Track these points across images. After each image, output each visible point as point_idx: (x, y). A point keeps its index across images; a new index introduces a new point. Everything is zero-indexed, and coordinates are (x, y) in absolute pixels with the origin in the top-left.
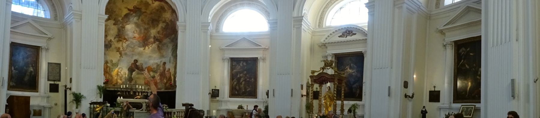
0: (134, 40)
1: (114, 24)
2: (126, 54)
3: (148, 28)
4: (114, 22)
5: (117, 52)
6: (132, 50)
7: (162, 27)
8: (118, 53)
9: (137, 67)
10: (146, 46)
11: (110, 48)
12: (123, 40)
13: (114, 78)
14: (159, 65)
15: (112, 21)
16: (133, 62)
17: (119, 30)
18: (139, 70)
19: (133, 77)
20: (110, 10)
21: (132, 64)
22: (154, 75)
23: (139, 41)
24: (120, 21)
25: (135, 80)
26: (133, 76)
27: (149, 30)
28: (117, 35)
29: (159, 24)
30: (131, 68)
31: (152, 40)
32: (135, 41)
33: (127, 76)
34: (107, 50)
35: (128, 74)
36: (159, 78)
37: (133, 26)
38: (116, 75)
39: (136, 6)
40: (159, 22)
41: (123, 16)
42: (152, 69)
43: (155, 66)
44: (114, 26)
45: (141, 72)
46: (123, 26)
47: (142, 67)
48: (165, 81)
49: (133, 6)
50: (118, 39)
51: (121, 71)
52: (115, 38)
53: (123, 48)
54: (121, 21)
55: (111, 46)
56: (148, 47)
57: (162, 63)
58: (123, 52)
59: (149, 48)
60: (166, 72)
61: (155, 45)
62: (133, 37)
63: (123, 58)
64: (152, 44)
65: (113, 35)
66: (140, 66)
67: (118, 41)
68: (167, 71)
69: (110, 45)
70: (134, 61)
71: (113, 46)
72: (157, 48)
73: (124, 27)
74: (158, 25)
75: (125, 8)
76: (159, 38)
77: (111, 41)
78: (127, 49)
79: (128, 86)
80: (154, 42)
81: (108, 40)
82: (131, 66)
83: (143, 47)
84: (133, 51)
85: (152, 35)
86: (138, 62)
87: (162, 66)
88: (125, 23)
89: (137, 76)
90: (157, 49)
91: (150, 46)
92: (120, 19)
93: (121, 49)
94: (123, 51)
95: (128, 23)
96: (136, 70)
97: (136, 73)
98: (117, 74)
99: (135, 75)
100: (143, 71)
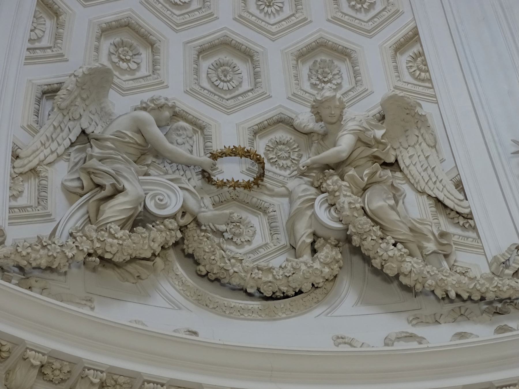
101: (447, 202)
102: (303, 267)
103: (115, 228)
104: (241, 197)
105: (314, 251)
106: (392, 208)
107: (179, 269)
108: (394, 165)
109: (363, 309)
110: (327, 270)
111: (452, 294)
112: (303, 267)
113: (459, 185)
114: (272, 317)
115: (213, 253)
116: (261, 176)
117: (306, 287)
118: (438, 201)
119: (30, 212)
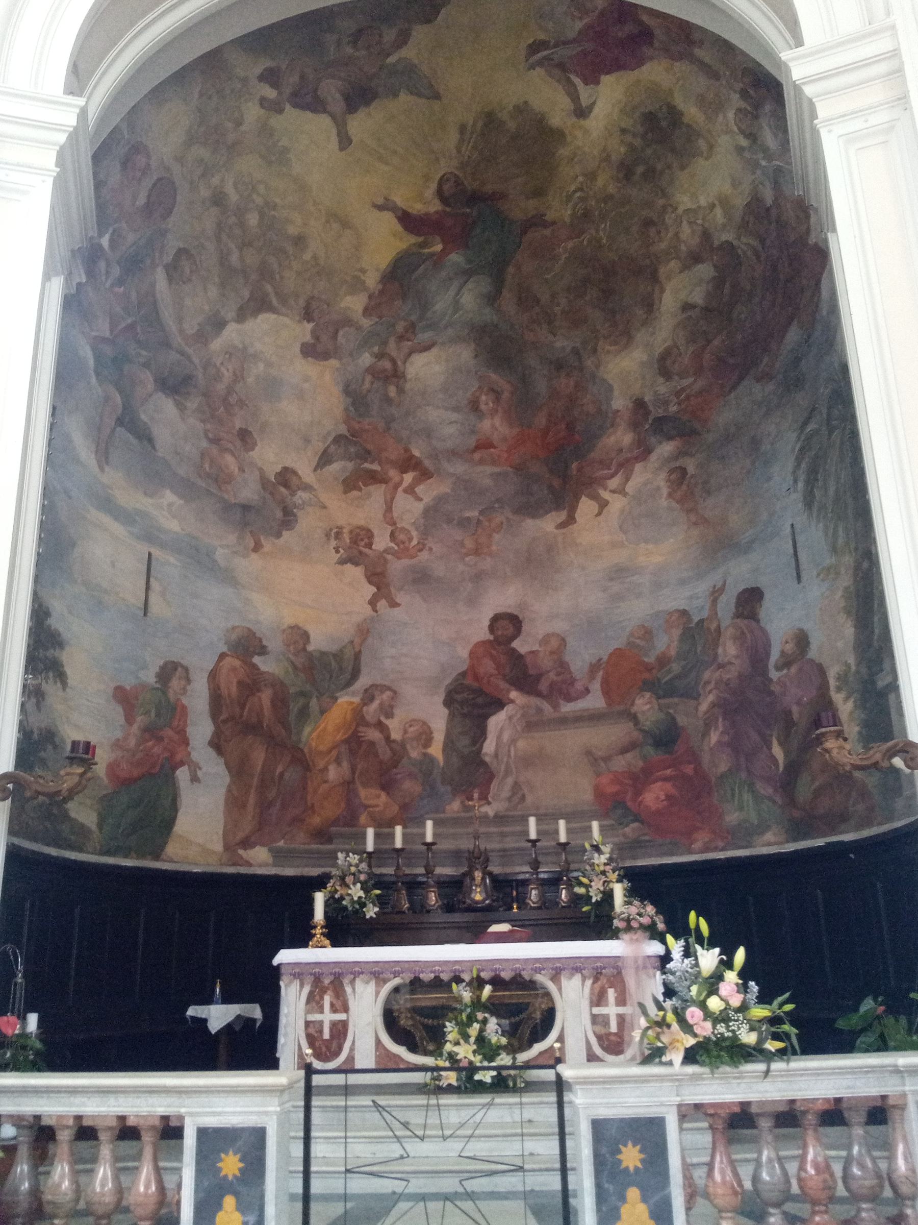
0: (481, 462)
1: (310, 351)
3: (576, 352)
5: (349, 566)
6: (469, 544)
8: (356, 573)
10: (577, 499)
11: (279, 535)
12: (393, 473)
13: (325, 769)
14: (702, 621)
15: (286, 320)
16: (481, 632)
18: (539, 694)
20: (253, 220)
21: (478, 651)
22: (673, 719)
23: (519, 469)
24: (359, 328)
25: (510, 781)
26: (489, 747)
27: (589, 363)
28: (338, 439)
29: (662, 291)
30: (468, 681)
32: (489, 469)
33: (436, 750)
34: (257, 547)
35: (448, 735)
36: (714, 737)
37: (465, 354)
38: (344, 748)
39: (458, 183)
40: (654, 277)
41: (372, 280)
42: (648, 668)
45: (556, 707)
46: (387, 365)
47: (563, 666)
48: (778, 751)
49: (434, 186)
50: (350, 465)
51: (390, 715)
52: (325, 459)
53: (392, 535)
54: (366, 323)
55: (288, 519)
56: (595, 497)
57: (727, 605)
58: (396, 567)
60: (774, 675)
62: (472, 442)
63: (396, 611)
64: (626, 466)
65: (307, 441)
66: (546, 662)
67: (350, 484)
68: (786, 662)
69: (279, 514)
70: (492, 628)
72: (665, 491)
73: (396, 376)
74: (650, 305)
75: (380, 208)
76: (673, 408)
77: (286, 477)
78: (430, 543)
80: (644, 451)
81: (261, 470)
82: (472, 672)
83: (558, 507)
84: (477, 552)
85: (620, 403)
86: (525, 627)
87: (728, 633)
88: (401, 338)
90: (670, 495)
91: (613, 492)
92: (354, 304)
93: (382, 542)
94: (398, 555)
95: (424, 336)
96: (514, 694)
97: (510, 718)
98: (347, 741)
99: (506, 737)
100: (569, 699)
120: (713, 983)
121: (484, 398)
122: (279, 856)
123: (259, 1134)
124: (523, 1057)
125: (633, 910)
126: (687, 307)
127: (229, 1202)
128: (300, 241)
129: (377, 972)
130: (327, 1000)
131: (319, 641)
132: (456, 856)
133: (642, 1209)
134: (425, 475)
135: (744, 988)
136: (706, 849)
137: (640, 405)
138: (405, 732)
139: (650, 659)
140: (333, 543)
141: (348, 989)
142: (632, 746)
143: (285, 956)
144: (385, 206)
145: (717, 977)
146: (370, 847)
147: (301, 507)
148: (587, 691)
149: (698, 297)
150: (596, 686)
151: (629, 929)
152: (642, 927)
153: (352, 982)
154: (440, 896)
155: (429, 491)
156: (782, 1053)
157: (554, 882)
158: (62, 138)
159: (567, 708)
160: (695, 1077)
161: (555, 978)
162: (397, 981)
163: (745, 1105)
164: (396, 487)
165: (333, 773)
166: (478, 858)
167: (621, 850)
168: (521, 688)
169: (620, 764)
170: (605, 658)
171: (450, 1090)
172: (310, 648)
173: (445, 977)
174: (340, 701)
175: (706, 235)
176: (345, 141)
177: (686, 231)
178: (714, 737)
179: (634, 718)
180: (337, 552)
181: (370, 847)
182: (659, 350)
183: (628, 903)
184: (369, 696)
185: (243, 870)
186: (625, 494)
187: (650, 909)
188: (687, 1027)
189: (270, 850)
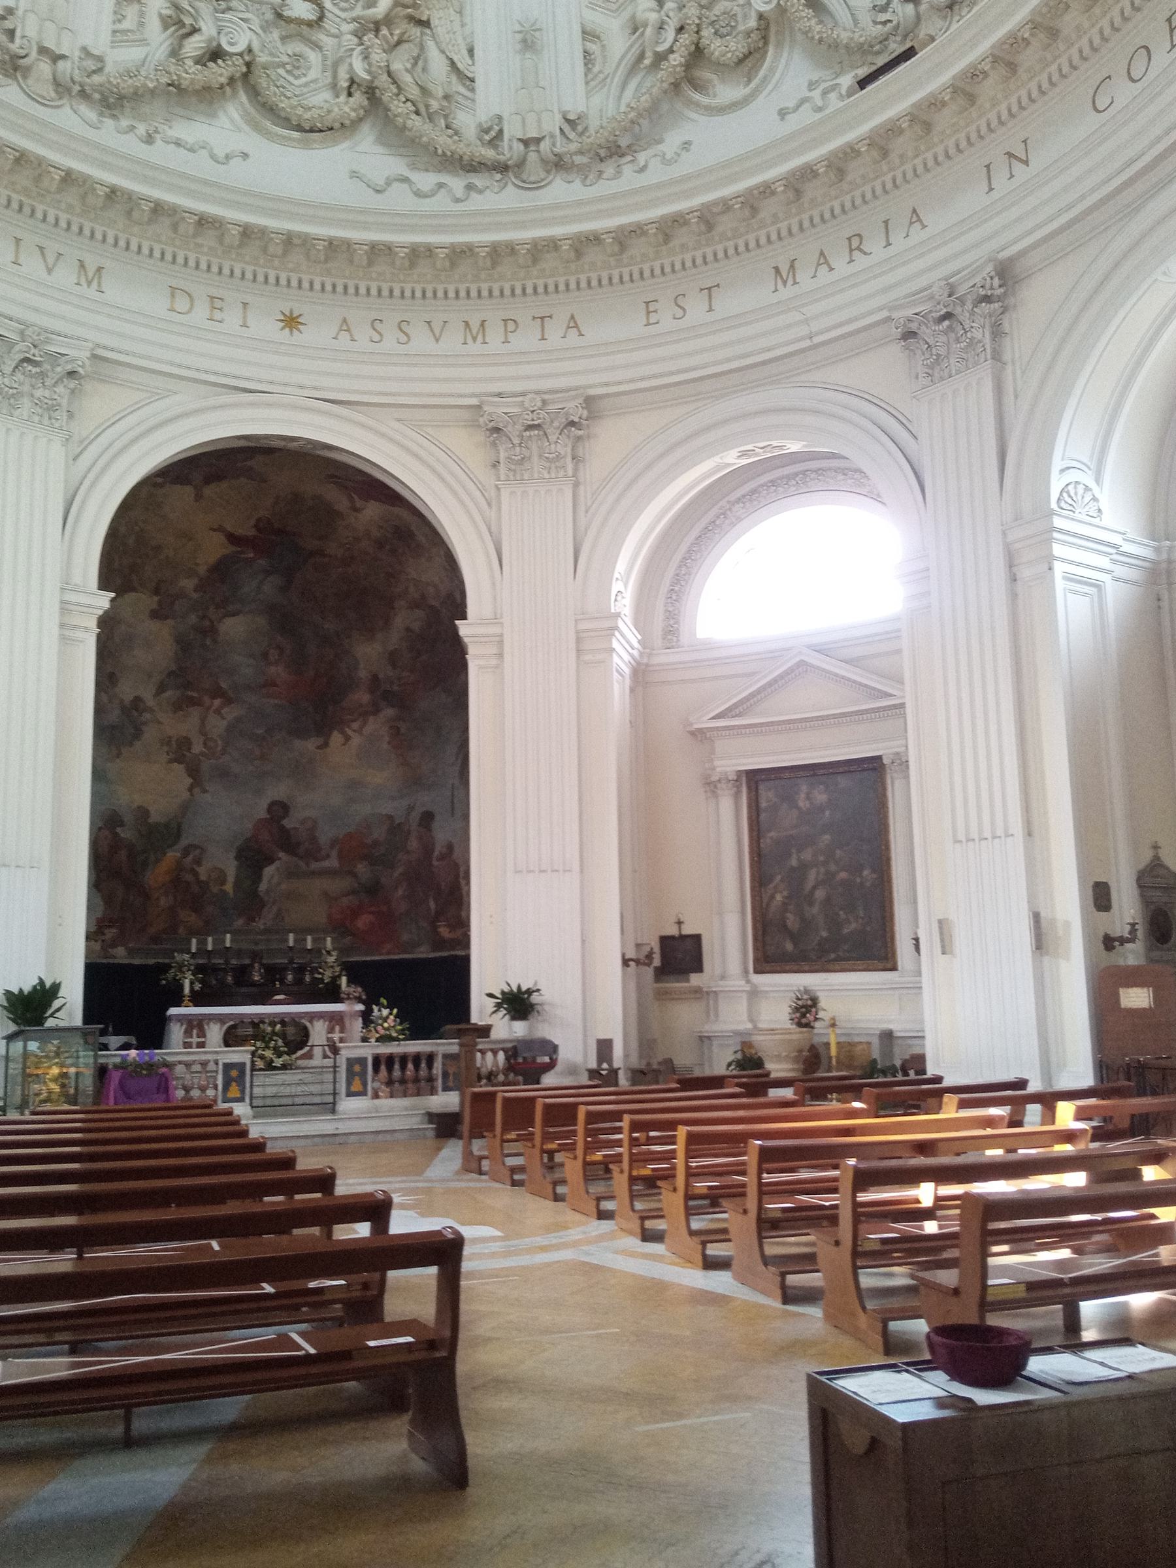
1: (155, 615)
2: (224, 774)
4: (153, 602)
7: (408, 629)
8: (179, 768)
9: (287, 842)
11: (131, 745)
12: (206, 700)
13: (158, 899)
14: (399, 824)
15: (144, 596)
16: (262, 813)
17: (184, 645)
18: (296, 855)
19: (268, 891)
20: (131, 541)
25: (275, 909)
26: (263, 887)
28: (171, 674)
31: (363, 697)
32: (273, 701)
33: (229, 887)
34: (118, 755)
35: (237, 876)
36: (400, 892)
37: (262, 621)
41: (202, 570)
43: (379, 833)
44: (154, 626)
45: (307, 864)
46: (207, 623)
47: (313, 839)
48: (432, 905)
49: (252, 522)
52: (161, 689)
53: (205, 744)
54: (195, 596)
55: (138, 733)
56: (343, 732)
57: (415, 815)
58: (206, 766)
59: (348, 738)
60: (435, 863)
61: (376, 726)
63: (206, 795)
65: (150, 676)
67: (178, 706)
68: (442, 857)
70: (269, 810)
71: (150, 734)
72: (387, 739)
75: (214, 530)
76: (396, 688)
79: (232, 941)
80: (376, 711)
81: (122, 701)
85: (363, 674)
89: (283, 886)
91: (354, 731)
92: (188, 584)
93: (197, 748)
96: (281, 854)
97: (278, 869)
99: (275, 880)
101: (460, 65)
102: (336, 109)
103: (189, 62)
104: (304, 32)
105: (350, 95)
106: (407, 70)
107: (243, 97)
108: (426, 24)
109: (380, 149)
110: (353, 114)
111: (440, 152)
112: (336, 109)
113: (471, 51)
114: (306, 145)
115: (268, 88)
116: (321, 18)
117: (337, 125)
118: (453, 64)
119: (131, 36)
120: (385, 1020)
121: (272, 651)
122: (131, 952)
123: (244, 1064)
124: (294, 1056)
125: (351, 990)
126: (408, 629)
127: (234, 1084)
128: (158, 548)
129: (221, 1019)
130: (195, 1032)
131: (155, 818)
132: (239, 953)
133: (359, 1082)
134: (229, 701)
135: (395, 1021)
136: (389, 953)
137: (375, 678)
138: (210, 876)
139: (369, 841)
140: (165, 748)
141: (206, 1027)
142: (353, 892)
143: (173, 1011)
144: (221, 529)
145: (387, 1017)
146: (194, 950)
147: (145, 723)
148: (328, 856)
149: (416, 626)
150: (334, 853)
151: (349, 998)
152: (356, 998)
153: (208, 1024)
154: (234, 977)
155: (232, 712)
156: (403, 1040)
157: (301, 970)
158: (100, 612)
159: (315, 866)
160: (378, 1046)
161: (311, 1022)
162: (232, 1023)
163: (391, 1054)
164: (209, 708)
165: (163, 902)
166: (255, 956)
167: (343, 951)
168: (286, 851)
169: (345, 901)
170: (341, 837)
171: (261, 1070)
172: (151, 821)
173: (256, 1021)
174: (168, 855)
175: (423, 597)
176: (199, 497)
177: (412, 589)
178: (400, 892)
179: (355, 875)
180: (168, 754)
181: (194, 950)
182: (391, 648)
183: (348, 986)
184: (186, 851)
185: (111, 961)
186: (361, 734)
187: (359, 989)
188: (377, 1032)
189: (126, 949)
